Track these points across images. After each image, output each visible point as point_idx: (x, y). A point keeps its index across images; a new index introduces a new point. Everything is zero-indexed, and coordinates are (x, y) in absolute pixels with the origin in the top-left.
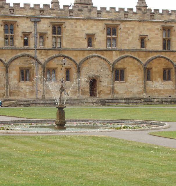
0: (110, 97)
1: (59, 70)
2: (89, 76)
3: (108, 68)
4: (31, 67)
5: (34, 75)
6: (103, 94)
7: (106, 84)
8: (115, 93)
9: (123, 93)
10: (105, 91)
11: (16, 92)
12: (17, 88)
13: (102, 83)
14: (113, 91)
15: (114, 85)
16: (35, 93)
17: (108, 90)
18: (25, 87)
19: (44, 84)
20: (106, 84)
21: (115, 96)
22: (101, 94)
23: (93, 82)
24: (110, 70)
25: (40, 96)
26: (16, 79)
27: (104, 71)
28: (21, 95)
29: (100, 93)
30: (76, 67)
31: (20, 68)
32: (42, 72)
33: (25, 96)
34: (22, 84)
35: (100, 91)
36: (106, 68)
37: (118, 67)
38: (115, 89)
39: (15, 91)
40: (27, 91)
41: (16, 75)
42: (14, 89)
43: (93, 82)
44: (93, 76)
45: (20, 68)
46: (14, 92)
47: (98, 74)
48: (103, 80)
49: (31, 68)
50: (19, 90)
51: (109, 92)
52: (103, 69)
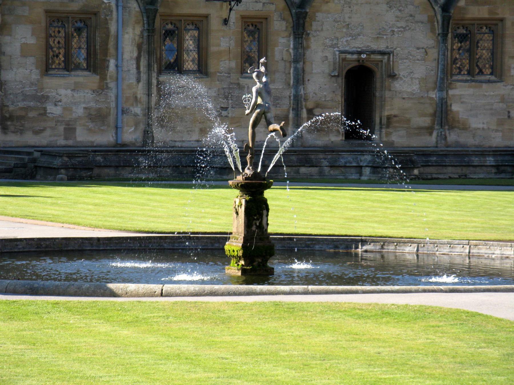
0: (430, 141)
1: (215, 24)
2: (341, 52)
3: (424, 18)
4: (96, 10)
5: (107, 44)
6: (402, 133)
7: (415, 87)
8: (452, 128)
9: (485, 126)
10: (408, 116)
11: (31, 114)
12: (34, 98)
13: (397, 85)
14: (443, 115)
15: (451, 92)
16: (112, 119)
17: (424, 115)
18: (70, 96)
19: (149, 84)
20: (415, 87)
21: (452, 137)
22: (390, 130)
23: (360, 84)
24: (433, 30)
25: (131, 135)
26: (31, 61)
27: (408, 34)
28: (52, 128)
29: (388, 126)
30: (287, 13)
31: (47, 12)
32: (142, 32)
33: (70, 130)
34: (62, 81)
35: (389, 118)
36: (418, 17)
37: (469, 16)
38: (455, 107)
39: (27, 109)
40: (79, 111)
41: (32, 41)
42: (21, 105)
43: (360, 84)
44: (360, 53)
45: (47, 12)
46: (22, 118)
47: (382, 46)
48: (402, 68)
49: (95, 14)
50: (45, 109)
51: (426, 121)
52: (403, 24)
